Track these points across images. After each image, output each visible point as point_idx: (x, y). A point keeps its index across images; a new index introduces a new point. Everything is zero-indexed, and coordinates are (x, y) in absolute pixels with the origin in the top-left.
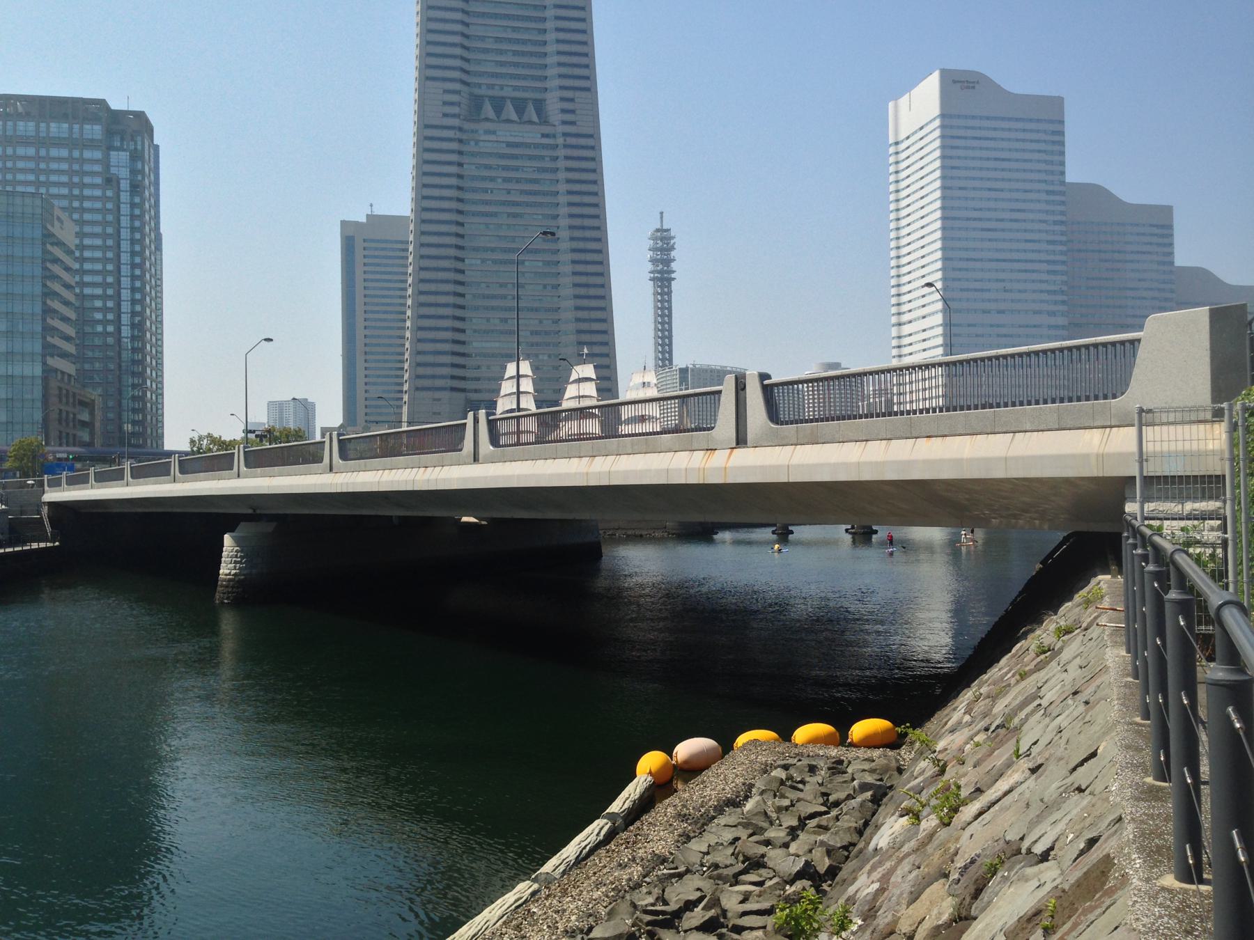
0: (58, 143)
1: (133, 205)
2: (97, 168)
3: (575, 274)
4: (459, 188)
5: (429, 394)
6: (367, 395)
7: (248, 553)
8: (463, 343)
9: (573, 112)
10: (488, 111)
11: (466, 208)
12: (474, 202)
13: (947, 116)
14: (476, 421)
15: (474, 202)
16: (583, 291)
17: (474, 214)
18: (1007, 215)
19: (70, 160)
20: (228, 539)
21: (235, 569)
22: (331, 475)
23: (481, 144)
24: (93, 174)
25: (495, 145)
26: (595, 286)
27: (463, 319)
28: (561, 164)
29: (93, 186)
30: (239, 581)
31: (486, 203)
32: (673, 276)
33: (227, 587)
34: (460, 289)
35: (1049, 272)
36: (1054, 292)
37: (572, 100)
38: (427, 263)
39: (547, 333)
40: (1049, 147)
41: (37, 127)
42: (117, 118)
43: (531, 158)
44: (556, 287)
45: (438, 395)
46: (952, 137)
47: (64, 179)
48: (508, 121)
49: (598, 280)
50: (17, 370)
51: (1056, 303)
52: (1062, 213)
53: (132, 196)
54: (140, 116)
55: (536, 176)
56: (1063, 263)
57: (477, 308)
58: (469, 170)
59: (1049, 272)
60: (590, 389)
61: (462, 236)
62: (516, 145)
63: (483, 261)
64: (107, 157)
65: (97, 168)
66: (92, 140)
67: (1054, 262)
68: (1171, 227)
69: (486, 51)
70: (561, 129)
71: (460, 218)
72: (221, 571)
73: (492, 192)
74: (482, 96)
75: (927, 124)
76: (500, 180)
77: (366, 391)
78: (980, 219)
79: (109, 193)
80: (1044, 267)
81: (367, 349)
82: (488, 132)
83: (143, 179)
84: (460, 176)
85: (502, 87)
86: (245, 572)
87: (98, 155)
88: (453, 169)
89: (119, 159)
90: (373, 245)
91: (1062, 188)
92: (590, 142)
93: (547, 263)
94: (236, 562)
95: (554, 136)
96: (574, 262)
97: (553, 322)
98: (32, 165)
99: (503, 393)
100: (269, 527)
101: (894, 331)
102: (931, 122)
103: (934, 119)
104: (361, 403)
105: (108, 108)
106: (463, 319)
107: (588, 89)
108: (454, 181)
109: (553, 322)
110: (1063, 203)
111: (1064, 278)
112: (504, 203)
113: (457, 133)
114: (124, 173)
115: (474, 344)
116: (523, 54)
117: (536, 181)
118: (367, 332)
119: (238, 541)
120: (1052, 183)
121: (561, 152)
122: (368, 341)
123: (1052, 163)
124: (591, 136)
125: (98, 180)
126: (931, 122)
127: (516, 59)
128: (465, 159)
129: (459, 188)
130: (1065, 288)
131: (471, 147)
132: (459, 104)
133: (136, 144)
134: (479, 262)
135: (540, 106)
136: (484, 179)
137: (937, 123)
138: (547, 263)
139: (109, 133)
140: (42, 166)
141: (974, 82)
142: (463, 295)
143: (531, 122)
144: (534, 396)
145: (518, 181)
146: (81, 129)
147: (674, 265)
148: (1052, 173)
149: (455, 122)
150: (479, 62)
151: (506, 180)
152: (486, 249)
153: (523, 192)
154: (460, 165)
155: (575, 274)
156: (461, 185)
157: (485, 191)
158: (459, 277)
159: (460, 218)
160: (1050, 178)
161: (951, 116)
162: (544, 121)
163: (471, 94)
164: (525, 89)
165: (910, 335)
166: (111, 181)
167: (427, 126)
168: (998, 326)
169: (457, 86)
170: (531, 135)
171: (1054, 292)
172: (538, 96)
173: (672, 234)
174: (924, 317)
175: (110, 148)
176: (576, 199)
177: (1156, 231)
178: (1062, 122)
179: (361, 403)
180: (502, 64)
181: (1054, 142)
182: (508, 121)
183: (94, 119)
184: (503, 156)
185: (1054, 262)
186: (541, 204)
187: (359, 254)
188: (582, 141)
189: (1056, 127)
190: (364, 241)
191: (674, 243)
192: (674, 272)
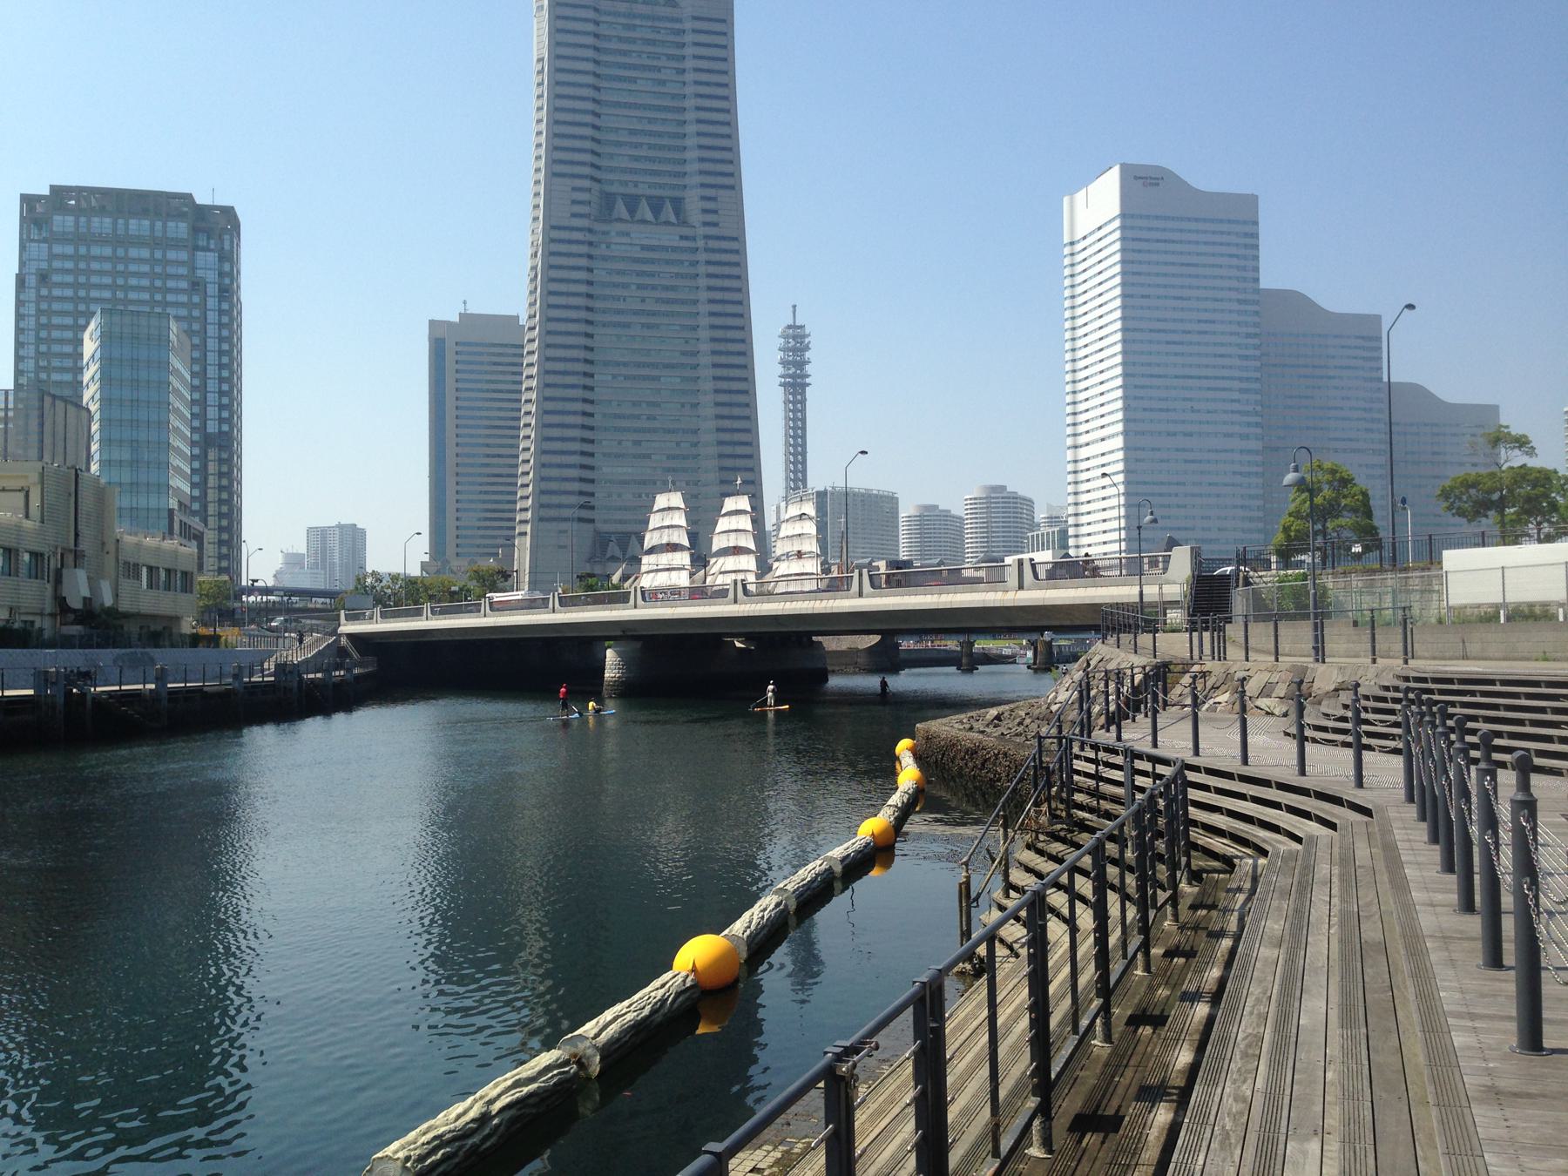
0: (139, 242)
1: (221, 312)
2: (183, 271)
3: (717, 391)
4: (589, 296)
5: (553, 526)
6: (458, 523)
7: (626, 661)
8: (592, 468)
9: (715, 212)
10: (621, 210)
11: (597, 317)
12: (604, 311)
13: (1129, 216)
14: (861, 575)
15: (604, 311)
16: (726, 411)
18: (1196, 327)
19: (152, 261)
23: (613, 247)
24: (178, 277)
26: (739, 405)
27: (592, 442)
28: (702, 269)
29: (177, 291)
31: (619, 312)
32: (808, 380)
34: (588, 408)
35: (1241, 391)
36: (1247, 413)
37: (713, 199)
39: (685, 457)
40: (1242, 252)
41: (115, 223)
42: (203, 212)
43: (668, 262)
44: (695, 406)
47: (145, 282)
48: (644, 222)
50: (143, 502)
52: (1256, 325)
54: (229, 213)
57: (606, 429)
59: (1241, 391)
60: (745, 523)
61: (592, 349)
63: (614, 376)
64: (192, 258)
65: (183, 271)
69: (619, 144)
70: (702, 231)
71: (589, 329)
72: (606, 675)
73: (624, 300)
74: (614, 194)
75: (1106, 224)
76: (634, 287)
77: (457, 519)
78: (1164, 331)
79: (196, 299)
80: (1236, 384)
81: (460, 470)
84: (590, 283)
85: (636, 185)
87: (183, 256)
88: (583, 275)
90: (466, 349)
91: (1256, 297)
93: (684, 379)
95: (694, 239)
96: (715, 378)
97: (691, 446)
98: (108, 266)
99: (651, 526)
100: (638, 645)
101: (1070, 455)
102: (1110, 221)
103: (1114, 219)
104: (451, 532)
107: (732, 187)
108: (583, 288)
109: (691, 446)
110: (1256, 313)
111: (1259, 397)
112: (636, 313)
113: (587, 234)
114: (211, 276)
115: (604, 469)
116: (661, 147)
117: (673, 288)
118: (459, 450)
119: (619, 654)
120: (1245, 291)
121: (702, 257)
122: (459, 460)
123: (1244, 268)
124: (735, 239)
125: (184, 285)
126: (1110, 221)
127: (652, 153)
129: (589, 296)
130: (1259, 408)
133: (223, 243)
134: (610, 378)
135: (677, 204)
136: (616, 285)
137: (1117, 223)
138: (684, 379)
139: (195, 230)
140: (120, 267)
141: (1158, 179)
142: (592, 415)
143: (667, 223)
144: (687, 530)
145: (654, 288)
146: (165, 227)
150: (611, 156)
151: (640, 287)
152: (618, 364)
153: (658, 300)
154: (590, 270)
155: (717, 391)
156: (590, 292)
157: (618, 298)
158: (588, 395)
159: (589, 329)
161: (1132, 216)
163: (602, 192)
164: (661, 186)
165: (1088, 459)
166: (197, 285)
168: (1184, 450)
169: (587, 183)
170: (669, 236)
171: (1247, 413)
172: (677, 194)
173: (807, 332)
174: (1103, 440)
175: (196, 248)
177: (1360, 342)
178: (1256, 223)
179: (451, 532)
180: (636, 159)
181: (1246, 246)
182: (644, 222)
183: (181, 216)
186: (679, 314)
187: (450, 357)
189: (1248, 229)
190: (457, 344)
191: (809, 342)
192: (808, 376)
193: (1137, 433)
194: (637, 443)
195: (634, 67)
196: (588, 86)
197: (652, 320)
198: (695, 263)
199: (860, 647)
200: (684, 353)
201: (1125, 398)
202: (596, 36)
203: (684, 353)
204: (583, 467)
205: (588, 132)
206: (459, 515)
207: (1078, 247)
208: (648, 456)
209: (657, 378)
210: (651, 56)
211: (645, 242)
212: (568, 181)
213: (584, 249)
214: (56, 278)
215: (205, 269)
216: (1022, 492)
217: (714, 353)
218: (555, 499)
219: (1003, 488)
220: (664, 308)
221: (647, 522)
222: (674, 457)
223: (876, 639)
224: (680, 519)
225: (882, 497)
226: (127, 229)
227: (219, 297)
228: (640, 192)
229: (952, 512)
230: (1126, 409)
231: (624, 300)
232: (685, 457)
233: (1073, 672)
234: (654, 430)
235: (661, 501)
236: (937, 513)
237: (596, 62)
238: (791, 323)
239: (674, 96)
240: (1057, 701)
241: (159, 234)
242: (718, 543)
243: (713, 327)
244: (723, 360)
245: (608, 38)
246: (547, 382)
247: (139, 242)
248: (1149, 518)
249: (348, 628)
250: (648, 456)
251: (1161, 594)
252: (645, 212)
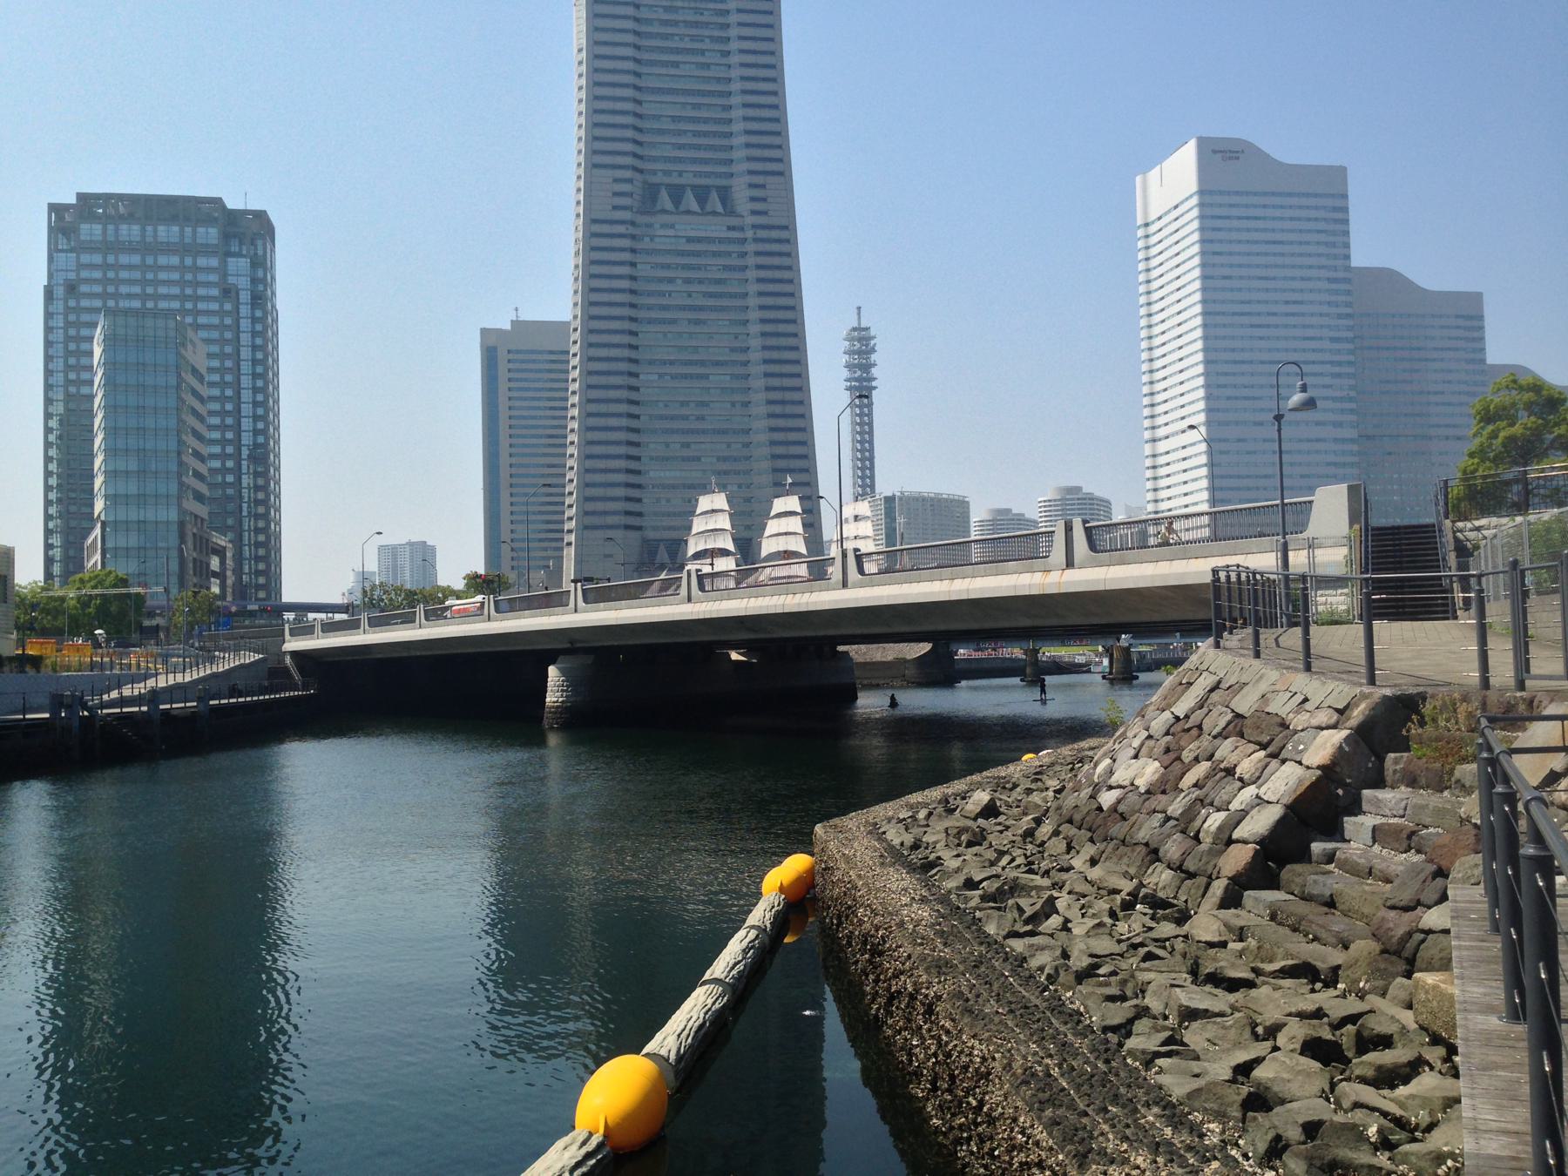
0: (168, 249)
1: (254, 320)
2: (213, 278)
3: (768, 389)
4: (632, 292)
5: (600, 534)
8: (638, 472)
9: (764, 200)
10: (665, 201)
11: (642, 314)
12: (650, 308)
13: (1206, 192)
15: (650, 308)
16: (778, 409)
17: (650, 321)
19: (182, 268)
20: (553, 671)
21: (562, 696)
22: (690, 605)
23: (657, 240)
24: (208, 284)
25: (673, 240)
26: (793, 403)
27: (637, 445)
28: (751, 261)
30: (566, 707)
32: (874, 384)
33: (555, 713)
34: (634, 410)
36: (1341, 399)
37: (763, 186)
38: (594, 380)
39: (736, 459)
40: (1331, 227)
41: (143, 230)
42: (234, 217)
43: (715, 254)
44: (746, 404)
45: (610, 533)
46: (1213, 217)
48: (688, 212)
49: (796, 396)
50: (150, 516)
51: (1342, 411)
52: (1349, 305)
53: (252, 309)
54: (261, 217)
55: (724, 276)
56: (1350, 363)
57: (654, 431)
58: (643, 270)
60: (795, 524)
61: (636, 348)
62: (699, 240)
63: (661, 376)
64: (224, 263)
65: (213, 278)
66: (207, 245)
67: (1339, 364)
68: (1481, 318)
69: (661, 132)
70: (750, 220)
71: (633, 327)
72: (548, 700)
73: (670, 295)
75: (1182, 202)
77: (512, 531)
79: (228, 307)
80: (1328, 368)
82: (663, 226)
84: (633, 278)
85: (680, 174)
86: (572, 700)
87: (214, 262)
90: (521, 357)
92: (784, 234)
94: (562, 691)
95: (742, 229)
96: (766, 375)
97: (743, 446)
98: (137, 275)
99: (694, 531)
100: (589, 659)
101: (1148, 450)
102: (1187, 199)
103: (1191, 196)
105: (224, 206)
106: (637, 445)
107: (781, 174)
108: (625, 284)
109: (743, 446)
110: (1349, 293)
111: (1352, 382)
112: (683, 308)
113: (629, 227)
114: (243, 283)
116: (705, 134)
117: (719, 282)
119: (563, 672)
120: (1335, 269)
122: (514, 471)
123: (1334, 245)
124: (786, 228)
125: (215, 292)
126: (1187, 199)
127: (696, 141)
128: (638, 258)
129: (632, 292)
130: (1353, 394)
131: (646, 244)
132: (630, 195)
133: (256, 249)
134: (656, 377)
135: (725, 194)
136: (660, 280)
137: (1195, 201)
138: (734, 377)
139: (226, 237)
140: (150, 276)
141: (1237, 152)
142: (637, 417)
143: (714, 213)
144: (732, 534)
145: (701, 281)
146: (194, 232)
147: (874, 371)
148: (1336, 257)
149: (626, 215)
150: (653, 145)
151: (687, 281)
152: (664, 363)
154: (633, 265)
155: (768, 389)
157: (662, 294)
158: (634, 396)
159: (633, 327)
160: (1331, 262)
161: (1211, 193)
162: (730, 211)
163: (645, 182)
164: (708, 175)
165: (1168, 453)
166: (228, 292)
167: (595, 221)
169: (628, 174)
170: (715, 228)
171: (1341, 399)
173: (872, 334)
175: (229, 254)
176: (770, 301)
177: (1461, 322)
178: (1345, 196)
180: (681, 147)
181: (1336, 221)
183: (209, 221)
184: (682, 253)
185: (1339, 364)
188: (774, 234)
189: (1338, 203)
190: (509, 352)
192: (875, 379)
193: (1220, 423)
194: (687, 445)
195: (678, 51)
196: (627, 72)
197: (703, 316)
198: (743, 255)
199: (909, 657)
200: (733, 350)
201: (1207, 386)
202: (637, 20)
203: (733, 350)
204: (629, 471)
205: (629, 120)
206: (513, 527)
207: (1153, 228)
208: (698, 459)
209: (705, 377)
210: (693, 38)
211: (692, 234)
212: (610, 172)
213: (626, 243)
214: (84, 288)
216: (1098, 493)
217: (765, 348)
218: (600, 506)
219: (1079, 489)
220: (711, 302)
221: (690, 528)
222: (725, 459)
223: (925, 647)
224: (724, 522)
225: (952, 501)
226: (155, 236)
227: (252, 304)
228: (682, 181)
229: (1027, 516)
230: (1208, 398)
231: (670, 295)
232: (736, 459)
233: (1150, 712)
234: (704, 432)
235: (705, 503)
236: (1010, 517)
237: (638, 48)
238: (856, 325)
239: (718, 80)
240: (1113, 781)
242: (768, 547)
243: (763, 321)
244: (775, 355)
245: (649, 22)
247: (168, 249)
248: (1297, 398)
249: (293, 644)
250: (698, 459)
251: (1312, 563)
252: (691, 202)
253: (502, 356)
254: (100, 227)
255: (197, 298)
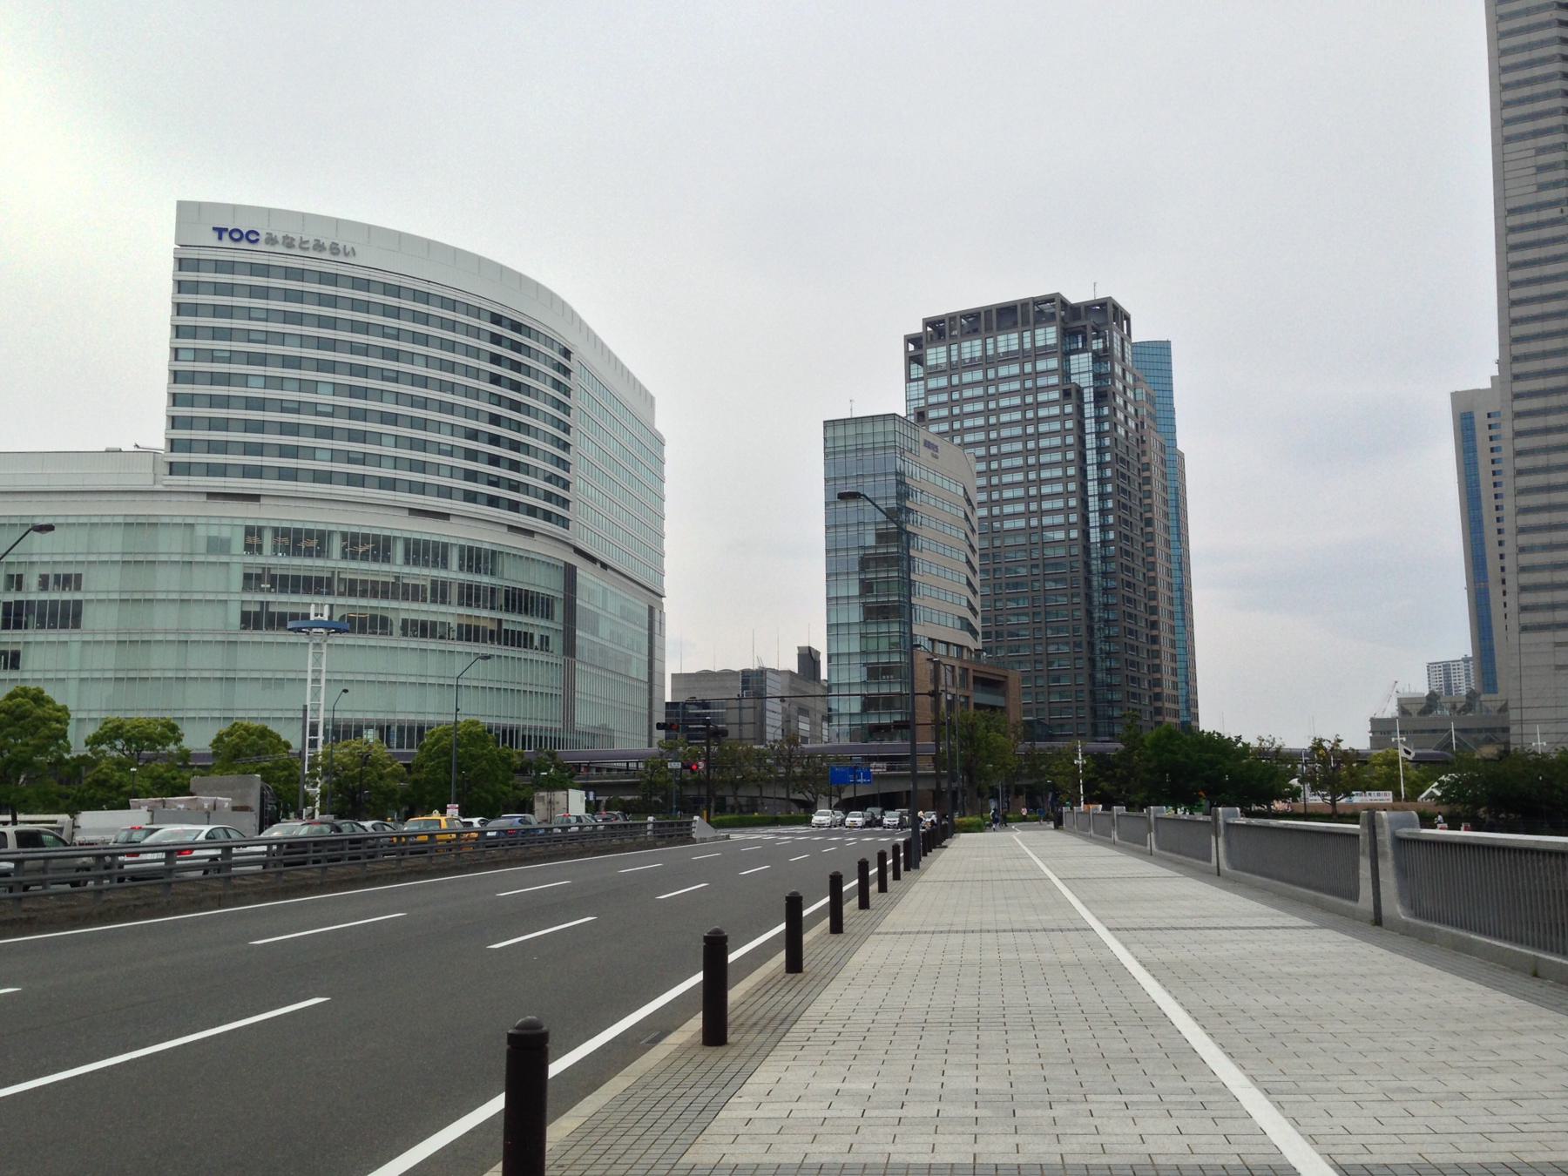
2: (1054, 380)
5: (1547, 636)
19: (1022, 376)
42: (1074, 311)
65: (1054, 380)
83: (1114, 383)
87: (1053, 363)
89: (1081, 364)
105: (1064, 304)
125: (1055, 395)
139: (1067, 333)
166: (1071, 393)
167: (1512, 212)
190: (1489, 415)
212: (1530, 143)
214: (932, 414)
215: (1079, 373)
241: (1027, 346)
246: (1516, 428)
247: (1009, 358)
253: (1481, 421)
254: (944, 349)
255: (1039, 405)
